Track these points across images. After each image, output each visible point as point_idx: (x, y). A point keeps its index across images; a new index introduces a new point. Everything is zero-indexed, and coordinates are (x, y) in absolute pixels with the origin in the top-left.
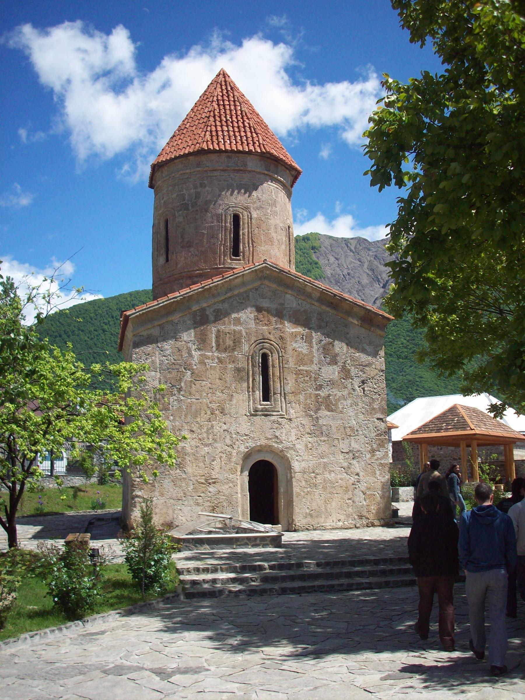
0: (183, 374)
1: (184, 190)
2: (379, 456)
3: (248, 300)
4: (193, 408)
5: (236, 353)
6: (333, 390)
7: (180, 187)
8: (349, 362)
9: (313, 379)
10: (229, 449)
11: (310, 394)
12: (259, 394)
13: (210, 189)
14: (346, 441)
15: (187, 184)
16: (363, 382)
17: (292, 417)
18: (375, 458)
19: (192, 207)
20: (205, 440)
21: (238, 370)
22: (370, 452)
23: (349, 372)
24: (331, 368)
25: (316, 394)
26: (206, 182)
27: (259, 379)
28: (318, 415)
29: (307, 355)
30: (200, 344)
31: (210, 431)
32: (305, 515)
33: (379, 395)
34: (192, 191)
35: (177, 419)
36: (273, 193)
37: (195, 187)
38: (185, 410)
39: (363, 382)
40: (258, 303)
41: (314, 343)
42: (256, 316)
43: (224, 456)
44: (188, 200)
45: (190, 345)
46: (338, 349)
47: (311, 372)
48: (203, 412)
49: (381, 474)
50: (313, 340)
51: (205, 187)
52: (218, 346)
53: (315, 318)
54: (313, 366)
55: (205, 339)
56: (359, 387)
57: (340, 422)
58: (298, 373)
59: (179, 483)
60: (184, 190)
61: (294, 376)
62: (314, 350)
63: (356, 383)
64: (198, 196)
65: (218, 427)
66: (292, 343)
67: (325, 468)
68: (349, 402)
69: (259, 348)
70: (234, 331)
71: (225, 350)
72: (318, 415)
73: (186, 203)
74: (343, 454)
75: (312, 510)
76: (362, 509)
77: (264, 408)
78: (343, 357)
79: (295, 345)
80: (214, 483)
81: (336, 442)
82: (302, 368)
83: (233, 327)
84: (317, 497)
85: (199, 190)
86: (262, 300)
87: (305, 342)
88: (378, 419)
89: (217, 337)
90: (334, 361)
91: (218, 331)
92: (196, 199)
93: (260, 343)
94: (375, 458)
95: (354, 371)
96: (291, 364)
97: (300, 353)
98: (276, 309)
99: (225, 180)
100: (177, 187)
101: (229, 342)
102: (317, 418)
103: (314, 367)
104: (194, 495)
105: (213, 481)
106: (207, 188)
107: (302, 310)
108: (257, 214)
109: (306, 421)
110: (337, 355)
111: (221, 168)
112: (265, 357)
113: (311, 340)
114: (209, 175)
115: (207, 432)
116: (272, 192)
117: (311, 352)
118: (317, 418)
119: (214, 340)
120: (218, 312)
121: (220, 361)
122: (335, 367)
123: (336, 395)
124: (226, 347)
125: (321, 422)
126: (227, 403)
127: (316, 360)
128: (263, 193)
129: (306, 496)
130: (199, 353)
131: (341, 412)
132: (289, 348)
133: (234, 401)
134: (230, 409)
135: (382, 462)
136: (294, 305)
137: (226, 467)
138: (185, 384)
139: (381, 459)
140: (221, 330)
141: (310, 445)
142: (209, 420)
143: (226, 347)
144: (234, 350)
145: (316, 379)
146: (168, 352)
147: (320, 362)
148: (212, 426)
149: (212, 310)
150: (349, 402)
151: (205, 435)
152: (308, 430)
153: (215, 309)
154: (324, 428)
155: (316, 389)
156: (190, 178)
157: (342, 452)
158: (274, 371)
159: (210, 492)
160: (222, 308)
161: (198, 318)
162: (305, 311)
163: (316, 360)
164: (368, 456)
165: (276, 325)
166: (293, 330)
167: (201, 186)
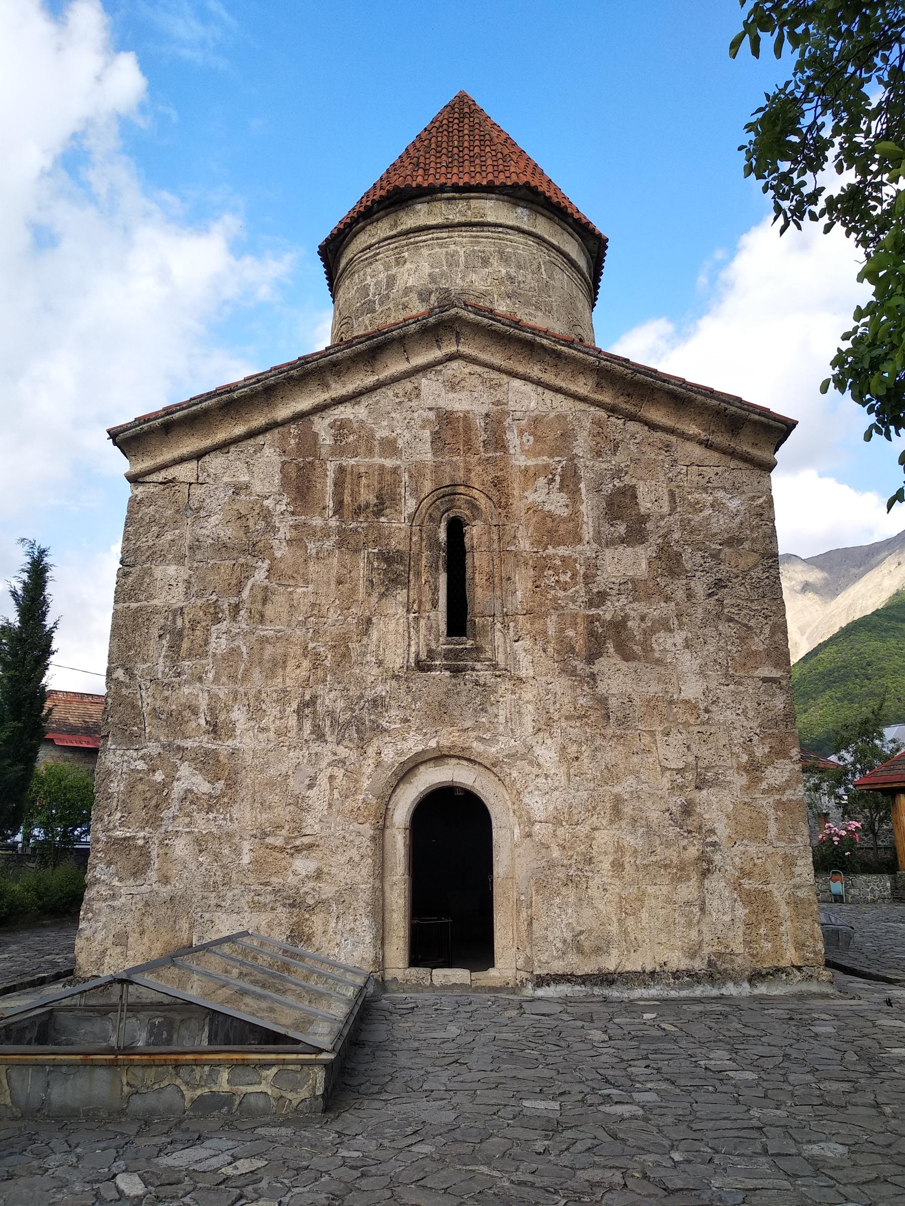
0: (248, 571)
1: (368, 277)
2: (771, 781)
3: (418, 396)
4: (269, 650)
5: (383, 519)
6: (635, 605)
7: (362, 273)
8: (676, 536)
9: (580, 579)
10: (353, 756)
11: (575, 616)
12: (440, 616)
13: (413, 266)
14: (676, 739)
15: (373, 266)
16: (719, 584)
17: (523, 674)
18: (764, 785)
19: (381, 304)
20: (293, 734)
21: (388, 558)
22: (747, 771)
23: (679, 562)
24: (629, 550)
25: (588, 616)
26: (406, 254)
27: (443, 579)
28: (595, 669)
29: (564, 520)
30: (295, 499)
31: (307, 711)
32: (559, 945)
33: (766, 617)
34: (381, 276)
35: (224, 679)
36: (543, 270)
37: (387, 268)
38: (245, 656)
39: (719, 584)
40: (441, 403)
41: (583, 491)
42: (437, 432)
43: (339, 773)
44: (374, 295)
45: (266, 503)
46: (649, 505)
47: (575, 560)
48: (291, 663)
49: (782, 832)
50: (582, 485)
51: (405, 262)
52: (339, 505)
53: (586, 433)
54: (579, 548)
55: (308, 488)
56: (710, 595)
57: (655, 688)
58: (541, 566)
59: (214, 846)
60: (368, 277)
61: (532, 573)
62: (583, 508)
63: (699, 588)
64: (391, 281)
65: (330, 699)
66: (526, 494)
67: (617, 812)
68: (679, 637)
69: (443, 508)
70: (382, 467)
71: (358, 511)
72: (595, 669)
73: (370, 300)
74: (668, 773)
75: (582, 932)
76: (731, 934)
77: (450, 650)
78: (662, 523)
79: (532, 497)
80: (310, 847)
81: (646, 739)
82: (551, 550)
83: (378, 460)
84: (593, 892)
85: (393, 271)
86: (451, 395)
87: (560, 490)
88: (765, 680)
89: (339, 484)
90: (636, 534)
91: (341, 470)
92: (388, 285)
93: (443, 496)
94: (764, 785)
95: (690, 559)
96: (524, 545)
97: (550, 515)
98: (487, 415)
99: (441, 246)
100: (357, 275)
101: (367, 496)
102: (593, 676)
103: (587, 549)
104: (251, 880)
105: (306, 840)
106: (408, 265)
107: (552, 415)
108: (507, 305)
109: (561, 684)
110: (644, 519)
111: (434, 222)
112: (456, 528)
113: (576, 484)
114: (412, 240)
115: (298, 712)
116: (539, 267)
117: (575, 515)
118: (593, 676)
119: (330, 489)
120: (342, 427)
121: (345, 540)
122: (640, 549)
123: (643, 618)
124: (359, 507)
125: (602, 688)
126: (355, 638)
127: (587, 532)
128: (519, 267)
129: (564, 890)
130: (291, 523)
131: (658, 662)
132: (518, 506)
133: (375, 634)
134: (364, 654)
135: (784, 799)
136: (533, 405)
137: (343, 803)
138: (252, 596)
139: (781, 789)
140: (349, 469)
141: (573, 749)
142: (306, 683)
143: (359, 507)
144: (379, 513)
145: (588, 579)
146: (213, 520)
147: (598, 536)
148: (314, 699)
149: (327, 421)
150: (679, 637)
151: (293, 721)
152: (568, 709)
153: (335, 421)
154: (613, 703)
155: (590, 604)
156: (379, 254)
157: (665, 769)
158: (478, 562)
159: (295, 873)
160: (352, 417)
161: (292, 442)
162: (561, 418)
163: (587, 532)
164: (742, 780)
165: (486, 451)
166: (530, 463)
167: (398, 263)
